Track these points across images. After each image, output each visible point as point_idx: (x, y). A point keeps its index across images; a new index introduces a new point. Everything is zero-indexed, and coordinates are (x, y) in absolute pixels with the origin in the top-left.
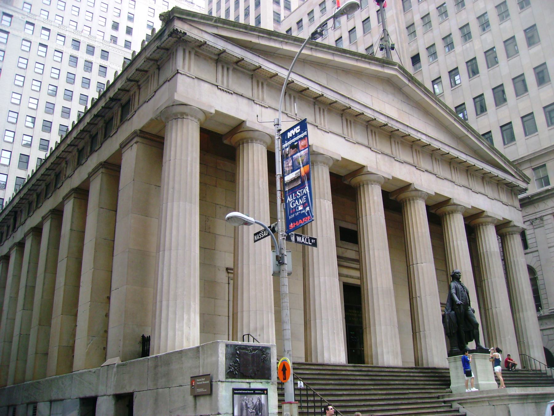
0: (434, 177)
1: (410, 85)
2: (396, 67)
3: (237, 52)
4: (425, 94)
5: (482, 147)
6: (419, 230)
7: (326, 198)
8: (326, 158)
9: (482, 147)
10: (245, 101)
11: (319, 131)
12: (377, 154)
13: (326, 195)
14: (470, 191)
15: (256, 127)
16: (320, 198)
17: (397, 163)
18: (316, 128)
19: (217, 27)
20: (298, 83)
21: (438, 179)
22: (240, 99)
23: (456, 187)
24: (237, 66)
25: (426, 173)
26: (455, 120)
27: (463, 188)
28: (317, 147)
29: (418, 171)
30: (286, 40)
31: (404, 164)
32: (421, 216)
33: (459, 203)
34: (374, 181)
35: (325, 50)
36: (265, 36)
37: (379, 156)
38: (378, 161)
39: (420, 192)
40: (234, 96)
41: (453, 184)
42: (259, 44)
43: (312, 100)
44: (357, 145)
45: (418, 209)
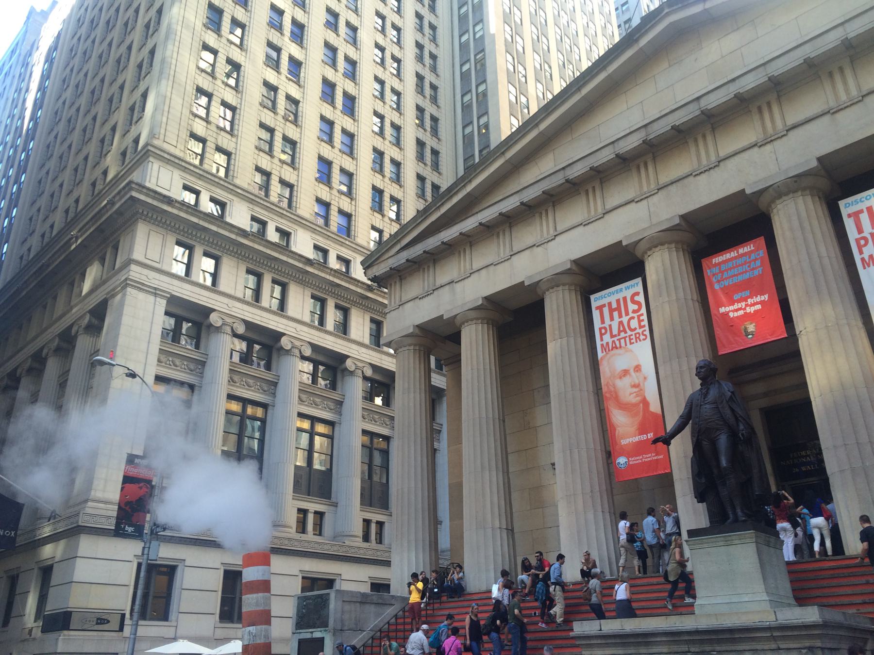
0: (826, 119)
2: (666, 11)
3: (417, 250)
8: (548, 280)
10: (447, 287)
11: (539, 248)
12: (649, 199)
17: (703, 176)
19: (399, 241)
25: (791, 133)
29: (768, 148)
34: (650, 249)
37: (655, 199)
38: (652, 209)
39: (771, 189)
40: (435, 292)
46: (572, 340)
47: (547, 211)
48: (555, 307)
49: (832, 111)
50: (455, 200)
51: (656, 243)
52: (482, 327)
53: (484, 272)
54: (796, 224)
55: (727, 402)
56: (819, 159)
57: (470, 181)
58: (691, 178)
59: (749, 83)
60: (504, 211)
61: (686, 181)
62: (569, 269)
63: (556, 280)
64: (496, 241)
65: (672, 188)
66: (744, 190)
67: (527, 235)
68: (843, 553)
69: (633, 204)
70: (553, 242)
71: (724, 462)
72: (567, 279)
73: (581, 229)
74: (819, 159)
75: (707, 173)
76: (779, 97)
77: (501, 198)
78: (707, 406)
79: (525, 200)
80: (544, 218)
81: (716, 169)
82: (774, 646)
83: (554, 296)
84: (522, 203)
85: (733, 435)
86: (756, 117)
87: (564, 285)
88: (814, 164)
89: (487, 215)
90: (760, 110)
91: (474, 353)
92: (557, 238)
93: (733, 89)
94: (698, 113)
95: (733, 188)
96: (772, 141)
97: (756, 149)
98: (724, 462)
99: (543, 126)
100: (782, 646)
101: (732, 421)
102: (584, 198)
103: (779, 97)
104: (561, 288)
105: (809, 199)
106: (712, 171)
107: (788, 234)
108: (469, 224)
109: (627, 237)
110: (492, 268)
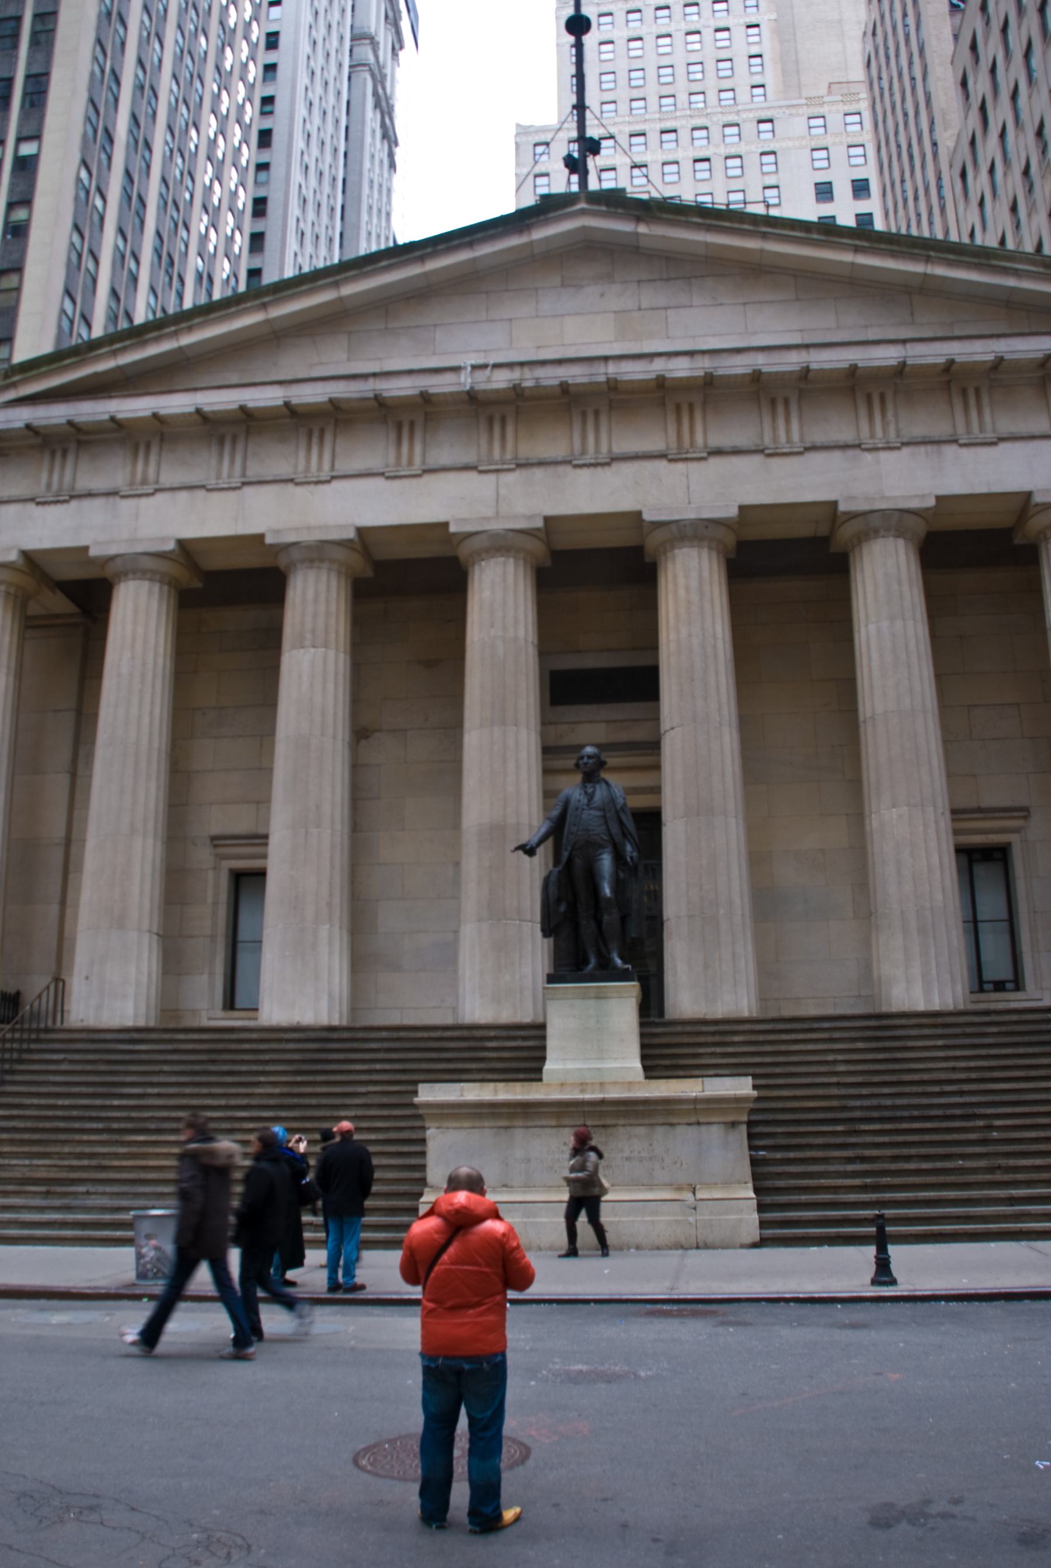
0: (757, 459)
1: (642, 229)
3: (56, 414)
4: (709, 228)
5: (1011, 282)
6: (672, 636)
7: (307, 643)
9: (1011, 282)
10: (99, 502)
11: (299, 490)
13: (308, 636)
14: (950, 450)
15: (112, 550)
16: (293, 647)
17: (585, 472)
18: (290, 486)
20: (216, 408)
21: (775, 462)
22: (86, 503)
23: (869, 457)
24: (78, 440)
26: (857, 250)
27: (906, 451)
28: (277, 532)
29: (680, 466)
30: (184, 325)
31: (615, 466)
32: (682, 592)
33: (866, 507)
35: (304, 288)
36: (127, 343)
37: (509, 478)
38: (503, 491)
39: (674, 527)
40: (74, 503)
41: (850, 453)
42: (119, 368)
43: (288, 420)
44: (427, 478)
45: (675, 576)
46: (331, 653)
47: (322, 432)
48: (310, 593)
49: (767, 452)
50: (152, 350)
51: (501, 544)
52: (161, 589)
53: (183, 496)
54: (694, 584)
55: (617, 812)
56: (742, 508)
57: (190, 329)
58: (569, 469)
59: (681, 369)
60: (250, 405)
61: (561, 469)
62: (350, 541)
63: (318, 553)
64: (215, 449)
65: (538, 473)
66: (639, 513)
67: (278, 459)
68: (661, 1012)
69: (473, 475)
70: (326, 488)
71: (607, 890)
72: (340, 554)
73: (380, 482)
74: (742, 508)
75: (592, 469)
76: (705, 403)
77: (235, 379)
78: (592, 812)
79: (295, 401)
80: (315, 440)
81: (606, 468)
82: (693, 1120)
83: (312, 574)
84: (287, 404)
85: (619, 857)
86: (671, 418)
87: (332, 561)
88: (733, 512)
89: (219, 400)
90: (678, 408)
91: (140, 630)
92: (335, 484)
93: (659, 366)
94: (602, 379)
95: (626, 504)
96: (686, 459)
97: (664, 463)
98: (607, 890)
99: (348, 290)
100: (701, 1120)
101: (618, 838)
102: (393, 436)
103: (705, 403)
104: (326, 565)
105: (714, 555)
106: (599, 469)
107: (682, 592)
108: (176, 404)
109: (459, 521)
110: (201, 493)
